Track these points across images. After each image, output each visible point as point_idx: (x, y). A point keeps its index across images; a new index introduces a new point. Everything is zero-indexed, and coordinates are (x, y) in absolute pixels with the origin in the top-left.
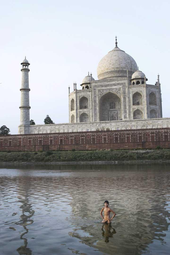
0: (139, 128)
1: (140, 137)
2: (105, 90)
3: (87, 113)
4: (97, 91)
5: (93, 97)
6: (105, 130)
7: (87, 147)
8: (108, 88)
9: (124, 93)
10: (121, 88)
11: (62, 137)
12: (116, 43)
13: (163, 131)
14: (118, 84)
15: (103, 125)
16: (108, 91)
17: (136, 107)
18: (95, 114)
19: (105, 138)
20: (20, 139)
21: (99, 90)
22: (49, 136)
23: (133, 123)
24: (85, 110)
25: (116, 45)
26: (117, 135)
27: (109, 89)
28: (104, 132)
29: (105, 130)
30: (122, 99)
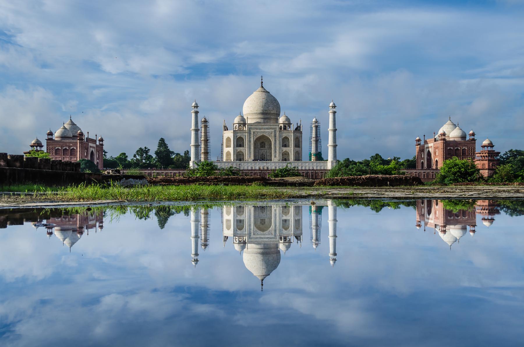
6: (266, 169)
8: (262, 131)
12: (262, 83)
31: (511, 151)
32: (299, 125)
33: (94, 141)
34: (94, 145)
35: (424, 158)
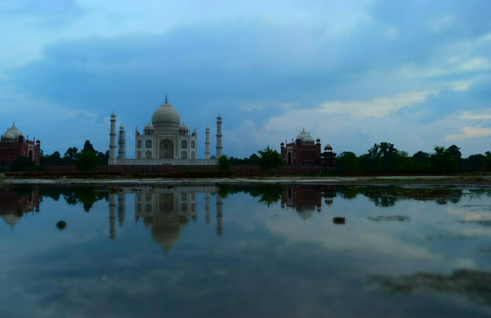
0: (188, 164)
2: (164, 137)
3: (151, 151)
4: (158, 137)
5: (155, 140)
8: (166, 135)
9: (176, 140)
10: (174, 136)
12: (166, 99)
16: (165, 138)
17: (183, 149)
18: (157, 152)
19: (171, 170)
21: (160, 137)
23: (185, 161)
24: (150, 149)
25: (166, 100)
27: (167, 137)
29: (169, 164)
30: (175, 144)
31: (344, 152)
32: (194, 131)
33: (32, 143)
34: (33, 146)
35: (286, 157)
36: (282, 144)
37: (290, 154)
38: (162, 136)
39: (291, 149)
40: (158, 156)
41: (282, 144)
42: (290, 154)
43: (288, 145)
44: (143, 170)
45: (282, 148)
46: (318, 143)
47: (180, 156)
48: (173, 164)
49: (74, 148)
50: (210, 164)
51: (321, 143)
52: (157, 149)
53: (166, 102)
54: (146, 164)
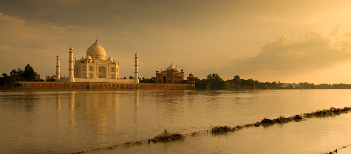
1: (122, 85)
4: (97, 64)
7: (104, 88)
8: (102, 64)
9: (108, 67)
11: (94, 84)
12: (96, 40)
13: (129, 84)
14: (106, 63)
15: (106, 80)
16: (101, 65)
17: (112, 73)
18: (96, 74)
20: (75, 84)
21: (98, 64)
22: (89, 83)
24: (92, 72)
25: (96, 41)
26: (115, 84)
28: (107, 83)
35: (161, 79)
36: (157, 71)
37: (165, 77)
38: (99, 64)
39: (166, 74)
40: (97, 77)
41: (157, 71)
42: (165, 77)
43: (162, 72)
44: (94, 85)
45: (157, 73)
46: (182, 71)
47: (110, 77)
48: (110, 82)
49: (19, 69)
50: (132, 82)
51: (183, 71)
52: (96, 72)
53: (96, 42)
54: (93, 82)
